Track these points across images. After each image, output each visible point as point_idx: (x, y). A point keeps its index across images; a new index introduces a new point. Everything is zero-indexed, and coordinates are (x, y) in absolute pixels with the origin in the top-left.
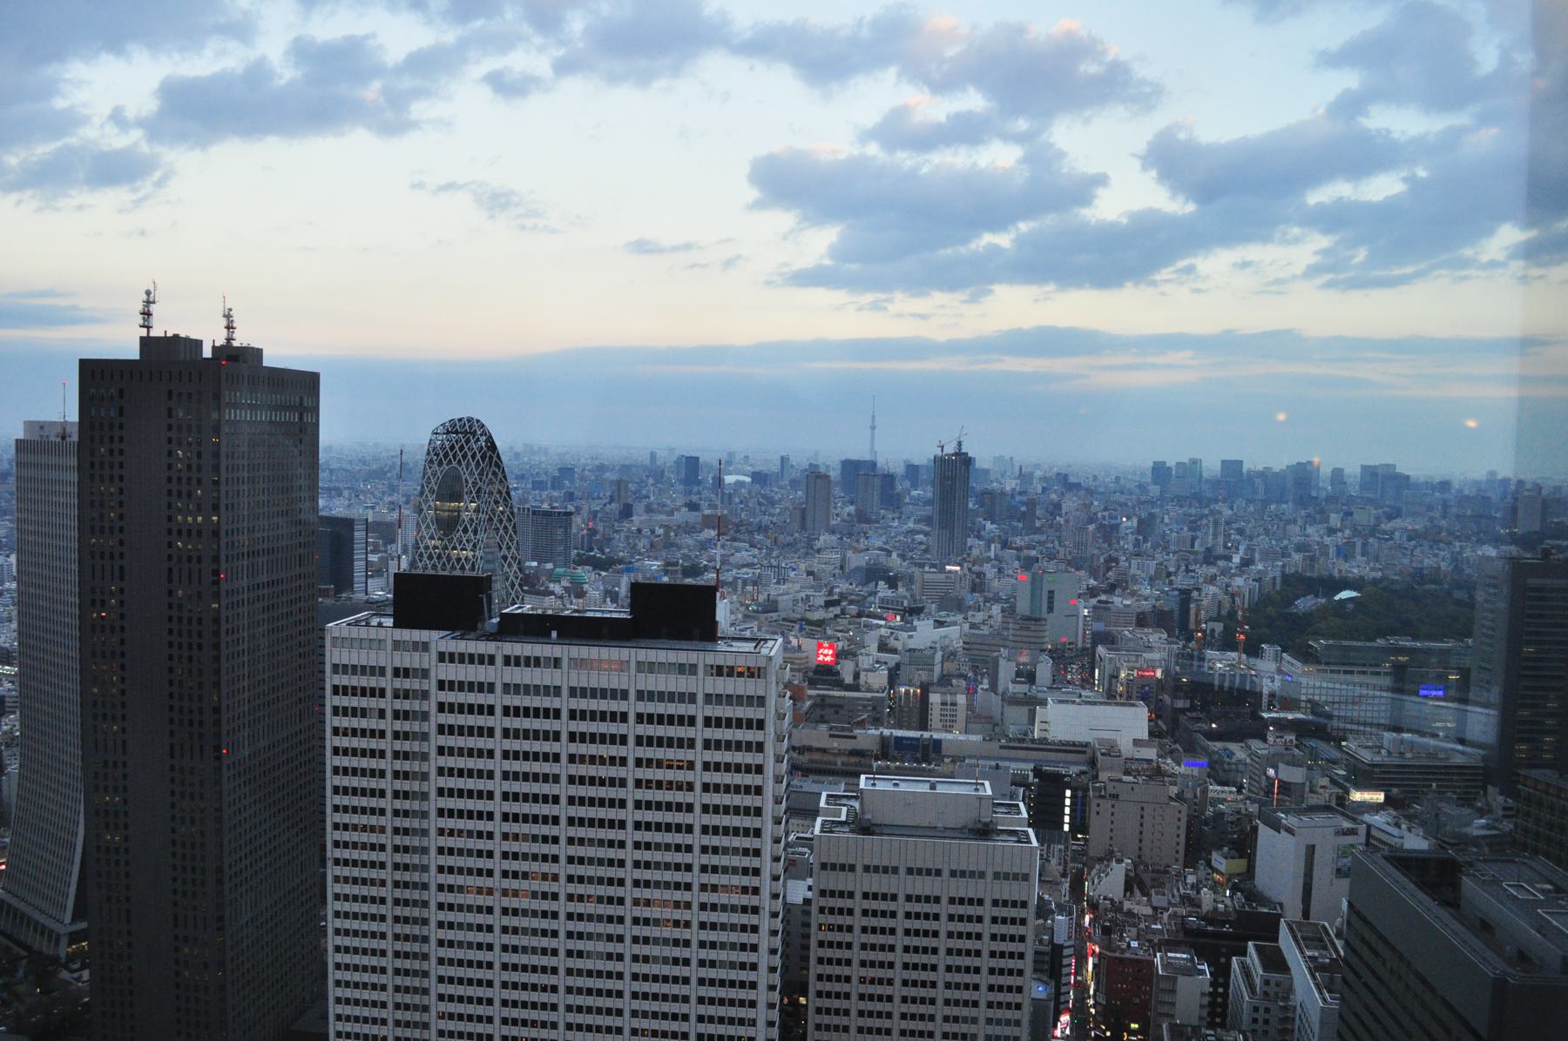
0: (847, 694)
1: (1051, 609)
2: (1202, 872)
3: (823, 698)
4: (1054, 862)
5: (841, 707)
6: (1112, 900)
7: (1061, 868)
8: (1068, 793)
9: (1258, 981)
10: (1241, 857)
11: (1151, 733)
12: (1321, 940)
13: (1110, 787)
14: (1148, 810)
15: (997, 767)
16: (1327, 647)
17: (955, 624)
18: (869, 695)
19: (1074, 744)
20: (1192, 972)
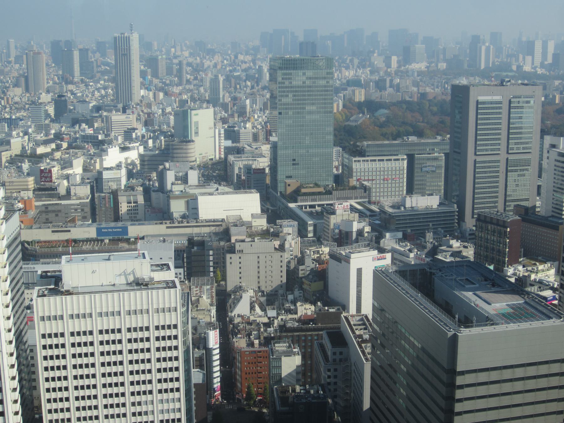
0: (63, 202)
1: (197, 133)
2: (297, 293)
3: (46, 206)
4: (205, 297)
5: (60, 211)
6: (242, 317)
7: (209, 301)
8: (211, 252)
9: (329, 353)
10: (320, 280)
11: (263, 211)
12: (364, 324)
13: (237, 245)
14: (262, 257)
15: (164, 241)
16: (368, 146)
17: (133, 148)
18: (78, 202)
19: (214, 221)
20: (289, 354)
